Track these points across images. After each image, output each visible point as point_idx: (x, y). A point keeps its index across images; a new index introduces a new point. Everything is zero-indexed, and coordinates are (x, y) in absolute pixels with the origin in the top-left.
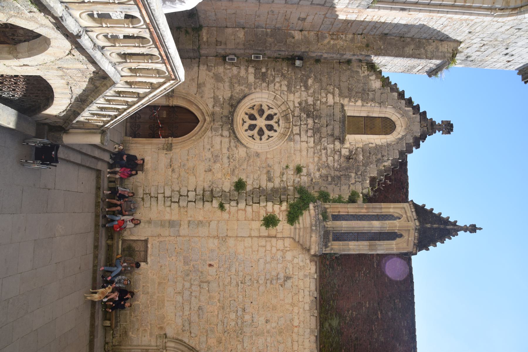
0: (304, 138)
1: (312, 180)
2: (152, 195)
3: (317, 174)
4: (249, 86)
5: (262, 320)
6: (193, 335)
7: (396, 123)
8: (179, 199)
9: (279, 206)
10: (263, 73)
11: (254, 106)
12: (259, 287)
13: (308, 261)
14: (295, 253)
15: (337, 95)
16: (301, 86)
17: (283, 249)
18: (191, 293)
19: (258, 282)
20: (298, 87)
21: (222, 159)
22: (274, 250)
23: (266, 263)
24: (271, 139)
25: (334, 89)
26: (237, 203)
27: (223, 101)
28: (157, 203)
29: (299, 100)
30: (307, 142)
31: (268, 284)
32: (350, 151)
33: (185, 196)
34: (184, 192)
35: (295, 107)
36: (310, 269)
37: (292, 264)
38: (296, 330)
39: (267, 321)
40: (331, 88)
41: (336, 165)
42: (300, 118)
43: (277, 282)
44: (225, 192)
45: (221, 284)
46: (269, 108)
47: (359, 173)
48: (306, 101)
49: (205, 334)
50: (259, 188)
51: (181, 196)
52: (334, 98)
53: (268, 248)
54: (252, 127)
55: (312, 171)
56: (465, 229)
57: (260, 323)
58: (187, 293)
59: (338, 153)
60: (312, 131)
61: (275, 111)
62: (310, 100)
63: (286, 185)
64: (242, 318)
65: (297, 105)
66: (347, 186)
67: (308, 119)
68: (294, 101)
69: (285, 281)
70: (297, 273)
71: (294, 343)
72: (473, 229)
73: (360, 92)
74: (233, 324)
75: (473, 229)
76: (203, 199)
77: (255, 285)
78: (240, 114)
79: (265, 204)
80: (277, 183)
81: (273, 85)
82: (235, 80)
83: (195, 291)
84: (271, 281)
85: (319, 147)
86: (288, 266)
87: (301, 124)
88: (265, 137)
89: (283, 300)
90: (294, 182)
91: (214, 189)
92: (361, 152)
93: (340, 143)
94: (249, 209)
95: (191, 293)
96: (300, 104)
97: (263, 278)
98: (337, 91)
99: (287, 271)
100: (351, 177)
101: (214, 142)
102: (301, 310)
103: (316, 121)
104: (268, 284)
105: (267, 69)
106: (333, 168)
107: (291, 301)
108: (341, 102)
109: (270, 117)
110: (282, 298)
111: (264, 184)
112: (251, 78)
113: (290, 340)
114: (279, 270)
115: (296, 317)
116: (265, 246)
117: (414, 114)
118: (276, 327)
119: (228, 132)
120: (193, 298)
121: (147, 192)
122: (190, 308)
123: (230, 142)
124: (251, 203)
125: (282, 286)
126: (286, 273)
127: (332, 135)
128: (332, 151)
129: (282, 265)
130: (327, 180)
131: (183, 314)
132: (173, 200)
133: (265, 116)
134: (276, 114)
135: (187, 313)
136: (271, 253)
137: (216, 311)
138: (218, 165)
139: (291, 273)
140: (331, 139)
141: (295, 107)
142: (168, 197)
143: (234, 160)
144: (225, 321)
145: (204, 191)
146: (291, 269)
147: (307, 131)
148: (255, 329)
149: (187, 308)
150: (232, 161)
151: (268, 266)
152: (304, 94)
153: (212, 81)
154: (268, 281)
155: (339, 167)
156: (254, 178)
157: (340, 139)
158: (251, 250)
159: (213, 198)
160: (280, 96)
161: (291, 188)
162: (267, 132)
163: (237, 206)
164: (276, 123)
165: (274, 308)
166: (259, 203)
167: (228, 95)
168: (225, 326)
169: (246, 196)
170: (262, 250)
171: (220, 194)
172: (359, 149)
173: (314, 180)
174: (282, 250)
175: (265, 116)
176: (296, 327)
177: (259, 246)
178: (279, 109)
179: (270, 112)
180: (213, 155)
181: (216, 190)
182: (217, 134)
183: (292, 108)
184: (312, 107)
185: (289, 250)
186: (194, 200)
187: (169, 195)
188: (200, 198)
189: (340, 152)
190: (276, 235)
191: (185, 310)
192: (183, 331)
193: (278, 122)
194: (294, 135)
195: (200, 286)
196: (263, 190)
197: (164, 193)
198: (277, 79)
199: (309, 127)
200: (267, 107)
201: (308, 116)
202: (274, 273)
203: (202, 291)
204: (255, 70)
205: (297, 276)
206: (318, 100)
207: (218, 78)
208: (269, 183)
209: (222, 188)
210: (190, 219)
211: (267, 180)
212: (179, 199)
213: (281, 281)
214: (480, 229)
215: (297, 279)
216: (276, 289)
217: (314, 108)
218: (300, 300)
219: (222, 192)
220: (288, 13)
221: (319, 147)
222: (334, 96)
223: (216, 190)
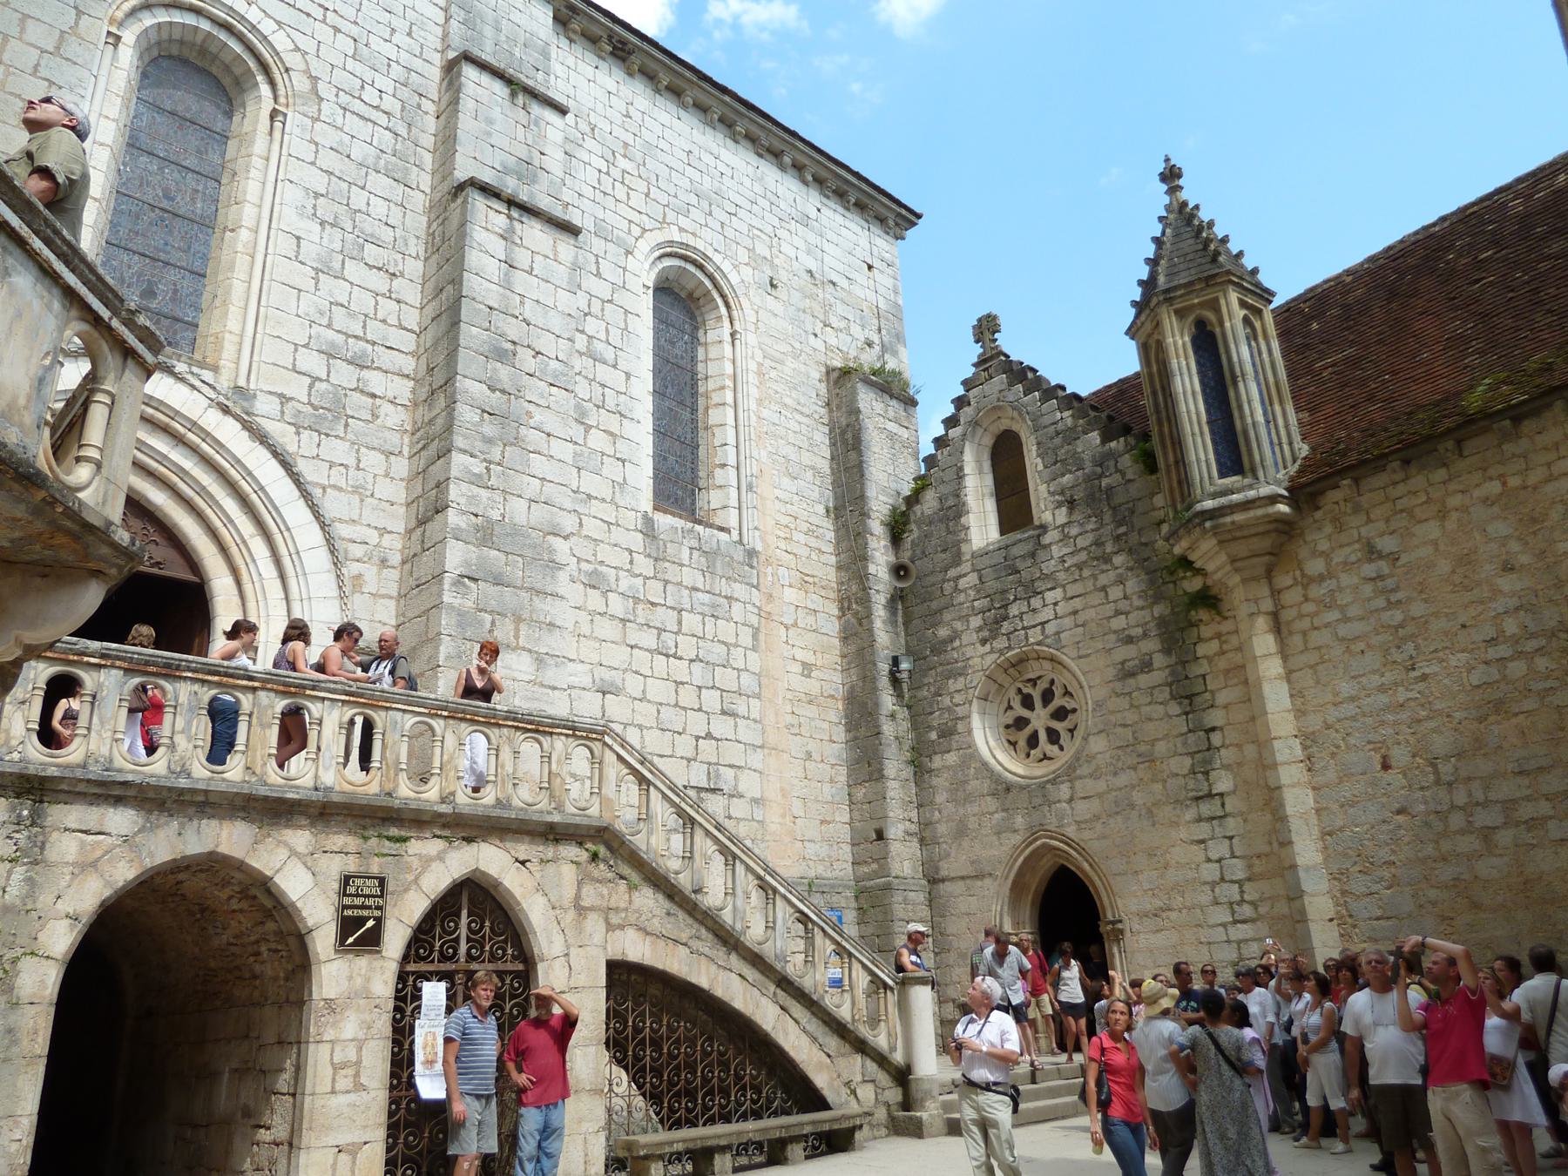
0: (1047, 614)
1: (1131, 569)
3: (1118, 560)
4: (964, 763)
5: (1507, 583)
7: (997, 432)
9: (1202, 628)
11: (1009, 742)
12: (1413, 619)
13: (1318, 515)
14: (1304, 552)
15: (959, 569)
16: (953, 649)
17: (1300, 588)
18: (1478, 804)
19: (1401, 626)
20: (956, 656)
21: (1120, 789)
22: (1309, 608)
23: (1346, 620)
24: (1069, 689)
25: (949, 580)
26: (1213, 729)
27: (1003, 810)
29: (978, 645)
30: (1055, 604)
31: (1400, 595)
32: (1059, 505)
33: (1221, 868)
34: (1210, 872)
35: (992, 651)
36: (1337, 503)
37: (1333, 549)
38: (1514, 482)
39: (1508, 568)
40: (948, 587)
41: (1090, 526)
42: (1011, 633)
43: (1391, 576)
44: (1193, 765)
45: (1433, 724)
46: (1010, 707)
47: (1099, 470)
48: (980, 629)
50: (1170, 685)
51: (1222, 879)
52: (965, 575)
53: (1305, 624)
54: (1054, 737)
55: (1112, 575)
56: (1173, 190)
57: (1518, 586)
58: (1483, 818)
59: (1066, 530)
60: (1033, 601)
61: (1012, 693)
62: (976, 622)
63: (1152, 624)
64: (1515, 640)
65: (988, 647)
66: (1130, 485)
67: (1011, 615)
68: (982, 656)
69: (1381, 556)
70: (1355, 532)
71: (1556, 473)
72: (1171, 176)
73: (948, 528)
74: (1542, 663)
75: (1171, 176)
77: (1410, 629)
78: (992, 761)
79: (1205, 662)
80: (1151, 645)
81: (957, 709)
82: (960, 794)
83: (1470, 795)
84: (1393, 591)
85: (1061, 576)
86: (1341, 560)
87: (1024, 628)
88: (1069, 704)
89: (1435, 543)
90: (1142, 608)
91: (1191, 794)
92: (1056, 482)
93: (1045, 532)
94: (1222, 698)
95: (1478, 804)
96: (984, 642)
97: (1386, 616)
98: (952, 573)
99: (1353, 558)
100: (1108, 485)
101: (1087, 817)
102: (1452, 487)
103: (1012, 598)
104: (1400, 595)
105: (931, 728)
106: (1097, 530)
107: (1432, 523)
108: (968, 557)
109: (1027, 702)
111: (1157, 677)
112: (952, 758)
113: (1549, 488)
114: (1356, 580)
115: (1477, 493)
116: (1304, 633)
117: (969, 404)
118: (1519, 539)
119: (1062, 786)
120: (1492, 796)
122: (1528, 798)
123: (1081, 778)
124: (1207, 696)
126: (1359, 560)
127: (1033, 555)
128: (1064, 545)
130: (1125, 534)
131: (1551, 818)
132: (1238, 898)
133: (1025, 713)
134: (1020, 691)
135: (1545, 808)
136: (1316, 614)
137: (1514, 721)
138: (1138, 797)
139: (1357, 546)
140: (1042, 555)
141: (992, 651)
143: (1118, 760)
144: (1541, 685)
145: (1200, 820)
146: (1347, 550)
147: (1034, 610)
148: (1541, 593)
149: (1526, 811)
150: (1120, 764)
151: (1353, 611)
152: (966, 638)
153: (966, 843)
154: (1393, 599)
155: (1094, 519)
156: (1150, 703)
157: (1039, 536)
158: (1320, 668)
159: (1214, 792)
160: (975, 687)
161: (1158, 610)
162: (1058, 702)
163: (1221, 729)
165: (1466, 560)
166: (1204, 676)
167: (991, 803)
168: (1556, 684)
169: (1193, 711)
170: (1316, 638)
171: (1200, 776)
172: (1052, 489)
173: (1131, 564)
174: (1305, 587)
175: (1025, 713)
176: (1504, 484)
177: (1306, 649)
178: (1007, 685)
179: (1016, 704)
180: (1117, 813)
181: (1192, 790)
182: (1069, 812)
184: (988, 614)
186: (1227, 842)
187: (1228, 912)
188: (1220, 826)
189: (1063, 526)
190: (1267, 613)
191: (1535, 815)
193: (1034, 682)
194: (1047, 637)
195: (1450, 784)
196: (1172, 673)
197: (1224, 925)
198: (946, 701)
199: (1025, 609)
201: (1005, 618)
202: (1368, 589)
203: (1463, 773)
204: (936, 753)
206: (973, 607)
207: (961, 831)
208: (1156, 665)
209: (1184, 776)
210: (1275, 845)
211: (1150, 671)
213: (1384, 566)
214: (1167, 160)
216: (1407, 573)
219: (1194, 773)
220: (789, 695)
222: (960, 576)
223: (1192, 790)
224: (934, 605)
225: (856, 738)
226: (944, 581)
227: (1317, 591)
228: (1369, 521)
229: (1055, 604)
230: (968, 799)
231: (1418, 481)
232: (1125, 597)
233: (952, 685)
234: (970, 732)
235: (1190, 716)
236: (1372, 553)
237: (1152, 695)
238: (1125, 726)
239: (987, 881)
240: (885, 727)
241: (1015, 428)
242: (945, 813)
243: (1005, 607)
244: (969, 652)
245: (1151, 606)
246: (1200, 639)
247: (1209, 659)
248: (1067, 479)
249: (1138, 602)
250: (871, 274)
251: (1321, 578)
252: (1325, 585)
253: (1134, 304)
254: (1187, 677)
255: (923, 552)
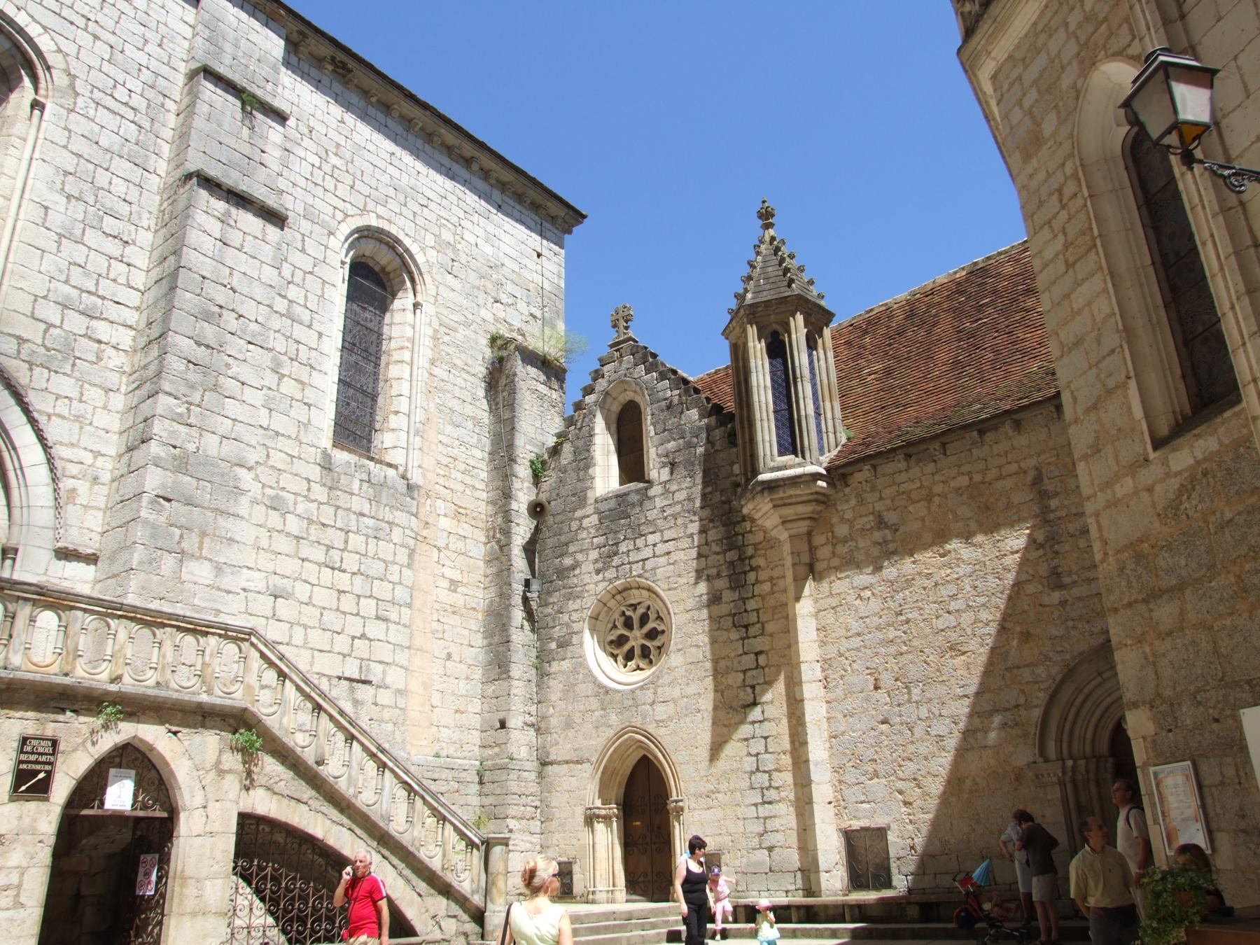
0: (647, 553)
2: (761, 829)
6: (1022, 701)
8: (765, 772)
9: (760, 572)
10: (559, 647)
13: (847, 490)
25: (576, 519)
28: (774, 817)
29: (593, 574)
30: (654, 545)
34: (750, 763)
35: (604, 580)
36: (860, 483)
37: (855, 519)
38: (977, 478)
40: (575, 525)
48: (596, 561)
49: (1016, 671)
51: (758, 769)
52: (588, 516)
62: (594, 555)
65: (601, 576)
67: (620, 552)
68: (596, 584)
69: (887, 526)
70: (871, 506)
71: (1004, 473)
72: (766, 216)
75: (766, 216)
76: (761, 722)
85: (660, 523)
86: (859, 527)
87: (629, 563)
89: (923, 520)
90: (718, 553)
92: (663, 447)
96: (598, 572)
98: (579, 513)
101: (664, 717)
102: (937, 478)
103: (622, 538)
105: (552, 639)
110: (919, 524)
112: (566, 665)
115: (953, 484)
117: (603, 377)
121: (756, 840)
125: (897, 530)
126: (872, 528)
129: (860, 540)
130: (710, 493)
134: (623, 613)
140: (647, 504)
141: (604, 580)
142: (763, 796)
143: (690, 674)
146: (865, 519)
148: (987, 563)
155: (688, 479)
157: (646, 489)
164: (635, 609)
169: (749, 638)
174: (834, 546)
182: (651, 713)
183: (606, 584)
184: (603, 549)
185: (833, 532)
186: (763, 740)
187: (759, 796)
189: (665, 482)
190: (805, 564)
192: (1016, 725)
193: (634, 607)
194: (646, 571)
197: (756, 805)
199: (631, 547)
201: (616, 554)
204: (554, 660)
205: (876, 505)
206: (592, 543)
207: (569, 724)
208: (724, 599)
212: (765, 772)
215: (881, 503)
217: (605, 546)
218: (918, 485)
220: (437, 606)
221: (660, 523)
224: (563, 538)
225: (490, 644)
226: (572, 520)
227: (842, 550)
228: (881, 498)
229: (654, 545)
231: (915, 471)
232: (707, 544)
233: (572, 605)
234: (581, 644)
235: (746, 641)
236: (881, 523)
237: (719, 622)
238: (697, 646)
239: (586, 765)
240: (514, 637)
241: (638, 399)
242: (558, 709)
243: (616, 544)
244: (587, 579)
245: (724, 552)
246: (757, 581)
247: (763, 597)
248: (671, 445)
249: (715, 548)
250: (539, 261)
251: (845, 541)
252: (847, 545)
253: (730, 311)
254: (746, 611)
255: (558, 495)
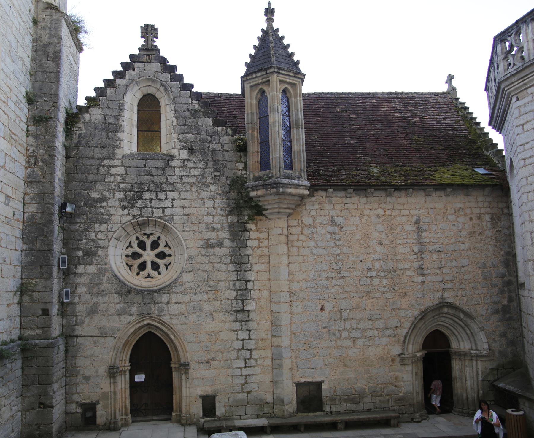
0: (168, 203)
1: (219, 194)
2: (243, 382)
3: (213, 188)
4: (101, 272)
5: (379, 249)
6: (399, 325)
7: (145, 93)
8: (247, 350)
10: (84, 255)
11: (127, 264)
12: (344, 253)
14: (304, 213)
15: (112, 162)
16: (101, 207)
17: (300, 228)
18: (353, 329)
19: (338, 255)
20: (102, 210)
21: (197, 302)
22: (302, 237)
23: (317, 247)
24: (169, 244)
25: (104, 166)
26: (249, 281)
27: (124, 303)
28: (253, 375)
29: (119, 209)
30: (173, 200)
31: (340, 243)
32: (183, 148)
33: (243, 343)
34: (239, 345)
35: (128, 214)
38: (388, 212)
39: (380, 244)
40: (102, 170)
41: (200, 166)
42: (143, 208)
44: (237, 296)
45: (342, 296)
46: (130, 246)
47: (209, 138)
48: (121, 200)
49: (397, 311)
50: (231, 256)
51: (243, 348)
52: (116, 166)
53: (300, 244)
54: (155, 267)
55: (208, 194)
56: (270, 20)
58: (354, 334)
59: (186, 163)
60: (159, 194)
61: (134, 239)
62: (120, 195)
63: (227, 225)
65: (126, 212)
67: (144, 198)
68: (121, 216)
69: (336, 225)
70: (327, 212)
72: (269, 12)
73: (107, 134)
74: (385, 281)
75: (269, 12)
76: (247, 321)
77: (342, 257)
79: (250, 249)
80: (224, 235)
81: (100, 242)
82: (95, 290)
83: (351, 325)
84: (337, 240)
85: (179, 186)
86: (320, 221)
87: (151, 207)
88: (167, 251)
89: (357, 226)
90: (222, 216)
91: (234, 309)
92: (183, 135)
93: (173, 160)
94: (255, 268)
95: (353, 329)
96: (124, 208)
97: (333, 249)
98: (106, 162)
99: (325, 222)
100: (213, 148)
102: (367, 206)
103: (146, 188)
104: (340, 243)
105: (79, 249)
107: (357, 218)
108: (120, 157)
109: (142, 245)
110: (355, 228)
111: (225, 251)
112: (92, 269)
113: (399, 219)
114: (324, 231)
115: (375, 212)
116: (299, 248)
117: (134, 70)
118: (386, 234)
119: (163, 295)
120: (359, 327)
121: (240, 388)
122: (370, 329)
123: (176, 293)
124: (249, 265)
125: (342, 228)
126: (327, 224)
127: (163, 169)
128: (183, 170)
129: (319, 228)
130: (219, 176)
131: (377, 337)
133: (140, 251)
135: (375, 333)
136: (305, 241)
137: (372, 300)
138: (206, 307)
139: (327, 217)
140: (168, 171)
142: (246, 363)
143: (198, 287)
144: (383, 289)
145: (236, 321)
146: (323, 218)
147: (159, 199)
148: (389, 256)
149: (369, 333)
150: (199, 289)
151: (320, 244)
152: (111, 203)
153: (96, 318)
154: (337, 244)
155: (202, 162)
157: (168, 160)
158: (303, 264)
159: (245, 309)
160: (114, 232)
161: (230, 219)
162: (161, 249)
163: (253, 281)
164: (148, 237)
165: (367, 236)
167: (116, 298)
168: (388, 290)
169: (241, 271)
170: (303, 251)
171: (239, 301)
172: (180, 138)
173: (220, 192)
174: (302, 228)
175: (140, 251)
176: (385, 212)
177: (298, 255)
178: (131, 234)
179: (135, 244)
180: (194, 313)
181: (235, 307)
182: (166, 309)
183: (130, 218)
184: (128, 193)
185: (302, 221)
186: (248, 332)
187: (243, 362)
188: (246, 325)
189: (184, 160)
190: (285, 235)
191: (372, 335)
192: (395, 336)
194: (165, 216)
195: (345, 320)
196: (233, 251)
197: (241, 368)
198: (92, 236)
199: (154, 197)
200: (129, 249)
201: (140, 198)
202: (328, 237)
203: (351, 317)
204: (81, 264)
205: (331, 212)
207: (93, 311)
208: (225, 245)
209: (232, 300)
210: (270, 336)
211: (221, 248)
212: (247, 350)
213: (336, 229)
215: (334, 211)
216: (345, 235)
217: (130, 191)
218: (356, 207)
219: (237, 299)
221: (179, 186)
222: (113, 166)
223: (235, 307)
224: (91, 178)
225: (31, 249)
226: (100, 165)
227: (306, 231)
228: (333, 209)
229: (173, 200)
230: (101, 293)
231: (355, 199)
232: (214, 208)
233: (97, 226)
234: (107, 256)
235: (239, 273)
236: (333, 222)
237: (221, 259)
238: (204, 271)
239: (109, 339)
240: (55, 246)
241: (158, 95)
242: (83, 299)
243: (142, 192)
244: (112, 211)
245: (227, 216)
246: (249, 238)
247: (253, 249)
248: (190, 136)
249: (220, 212)
251: (310, 226)
252: (311, 230)
253: (246, 64)
254: (240, 254)
255: (87, 143)
